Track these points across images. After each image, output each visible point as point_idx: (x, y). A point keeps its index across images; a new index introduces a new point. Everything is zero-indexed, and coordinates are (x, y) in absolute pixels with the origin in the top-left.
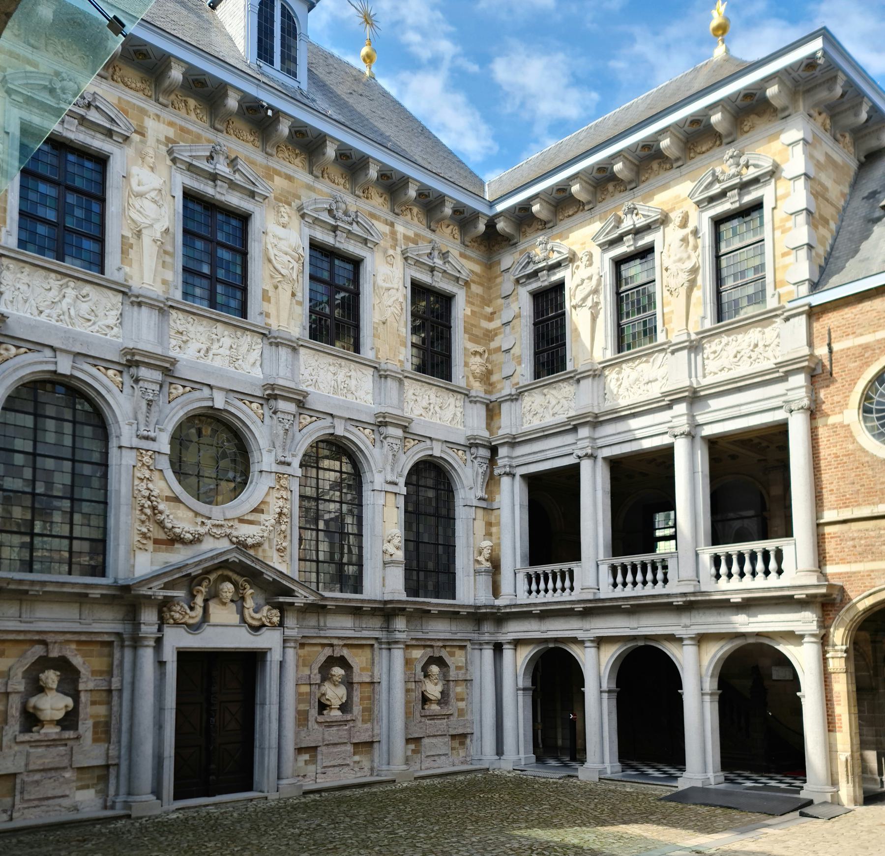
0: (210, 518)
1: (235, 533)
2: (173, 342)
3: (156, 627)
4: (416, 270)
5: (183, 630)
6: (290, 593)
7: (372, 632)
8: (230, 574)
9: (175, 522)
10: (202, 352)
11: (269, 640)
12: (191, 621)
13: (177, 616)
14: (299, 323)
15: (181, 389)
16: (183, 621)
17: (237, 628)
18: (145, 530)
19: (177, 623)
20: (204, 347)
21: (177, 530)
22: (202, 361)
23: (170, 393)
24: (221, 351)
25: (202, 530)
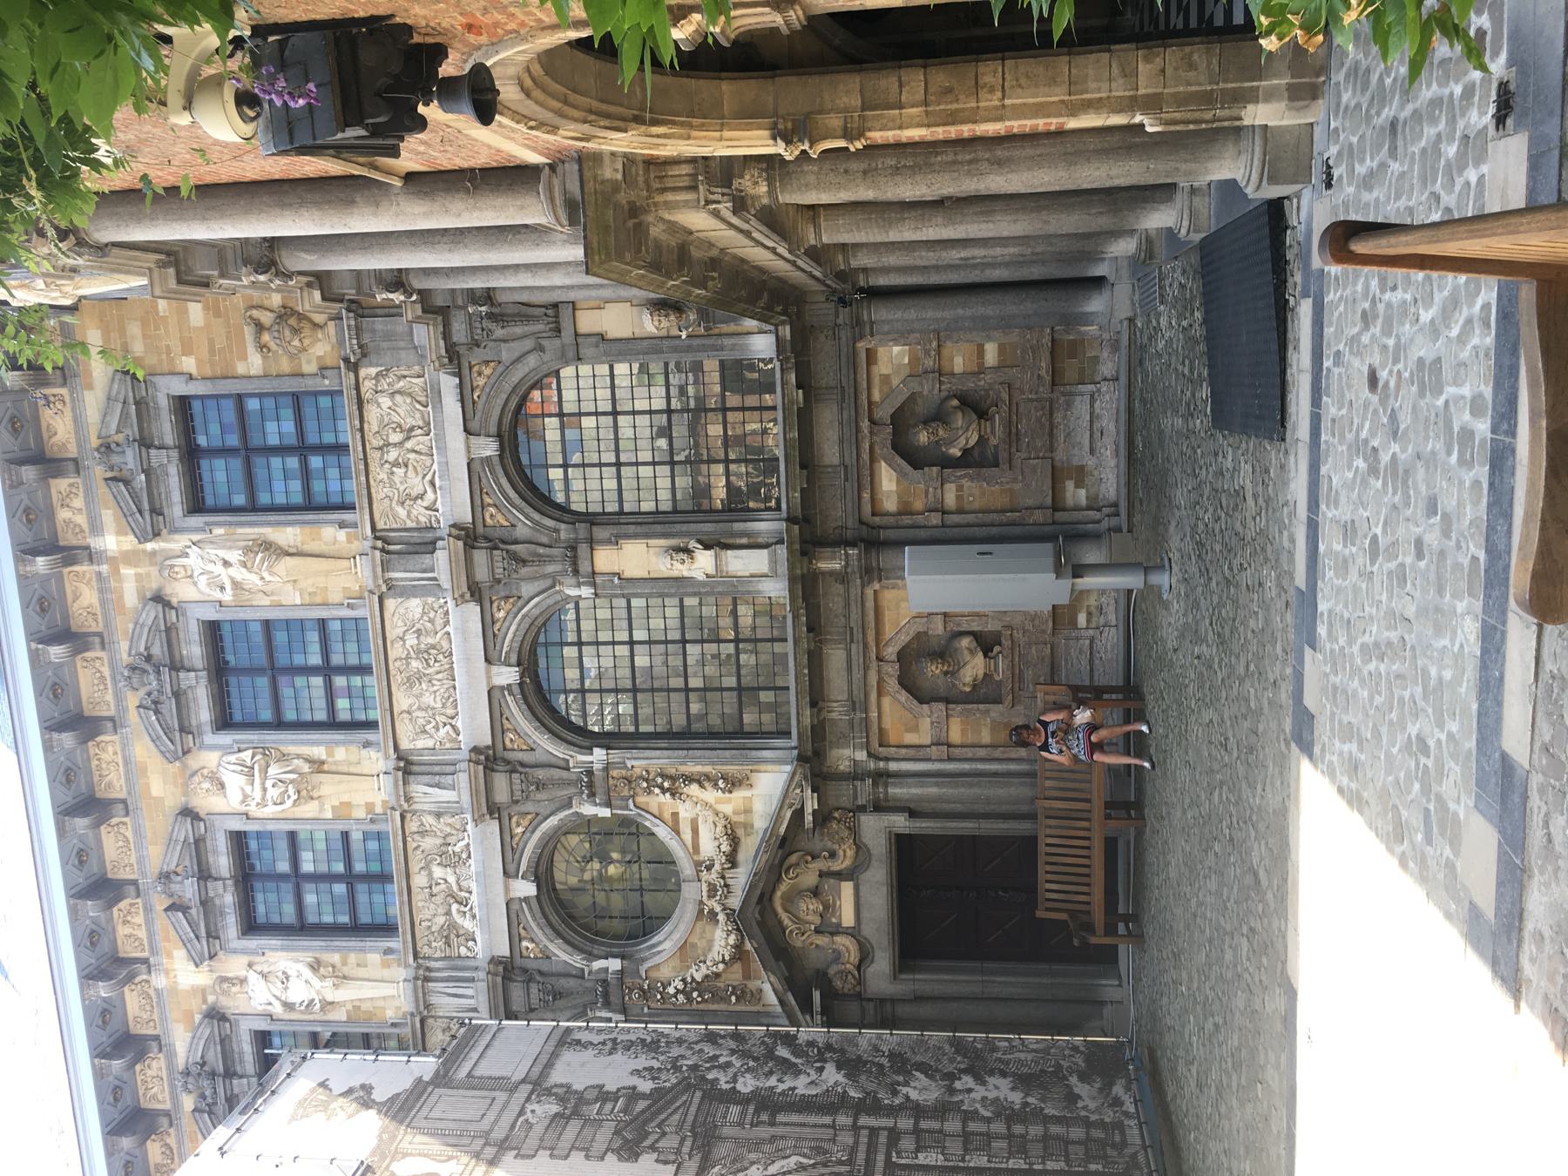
0: (701, 902)
1: (717, 867)
2: (463, 951)
3: (864, 1003)
4: (170, 506)
5: (870, 970)
6: (799, 814)
7: (853, 604)
10: (462, 908)
11: (876, 829)
14: (364, 752)
15: (525, 944)
17: (863, 889)
18: (733, 999)
20: (455, 907)
21: (727, 958)
22: (476, 910)
23: (536, 958)
24: (452, 879)
25: (721, 917)
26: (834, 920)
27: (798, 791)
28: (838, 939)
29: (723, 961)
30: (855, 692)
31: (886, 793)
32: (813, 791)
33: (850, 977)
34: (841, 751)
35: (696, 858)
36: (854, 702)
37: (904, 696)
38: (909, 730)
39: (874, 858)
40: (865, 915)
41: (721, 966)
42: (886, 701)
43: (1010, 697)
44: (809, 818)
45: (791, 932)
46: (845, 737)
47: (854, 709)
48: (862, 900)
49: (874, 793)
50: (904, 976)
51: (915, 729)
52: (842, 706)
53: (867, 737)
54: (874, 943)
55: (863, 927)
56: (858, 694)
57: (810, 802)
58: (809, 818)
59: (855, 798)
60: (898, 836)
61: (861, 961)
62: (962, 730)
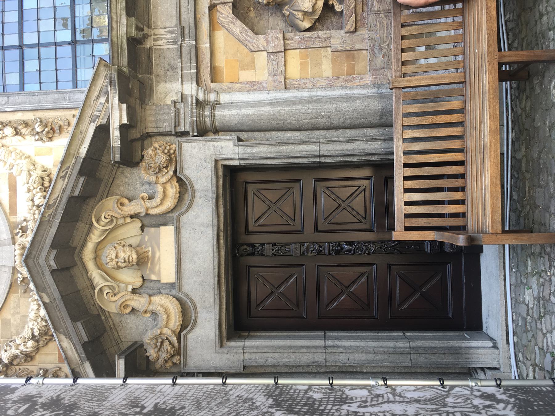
8: (90, 246)
9: (27, 333)
12: (175, 321)
13: (164, 355)
16: (174, 340)
19: (178, 352)
21: (36, 333)
26: (153, 277)
27: (103, 100)
28: (156, 299)
29: (33, 337)
30: (184, 16)
31: (213, 116)
32: (121, 101)
33: (166, 343)
34: (168, 85)
35: (12, 219)
36: (182, 29)
37: (238, 27)
38: (243, 68)
39: (198, 194)
40: (187, 266)
41: (30, 344)
42: (220, 35)
43: (353, 18)
44: (115, 135)
45: (101, 290)
46: (174, 69)
47: (182, 35)
48: (184, 247)
49: (199, 115)
50: (232, 343)
51: (251, 65)
52: (170, 32)
53: (198, 68)
54: (196, 300)
55: (184, 281)
56: (188, 19)
57: (116, 114)
58: (115, 135)
59: (177, 124)
60: (226, 168)
61: (184, 327)
62: (301, 64)
